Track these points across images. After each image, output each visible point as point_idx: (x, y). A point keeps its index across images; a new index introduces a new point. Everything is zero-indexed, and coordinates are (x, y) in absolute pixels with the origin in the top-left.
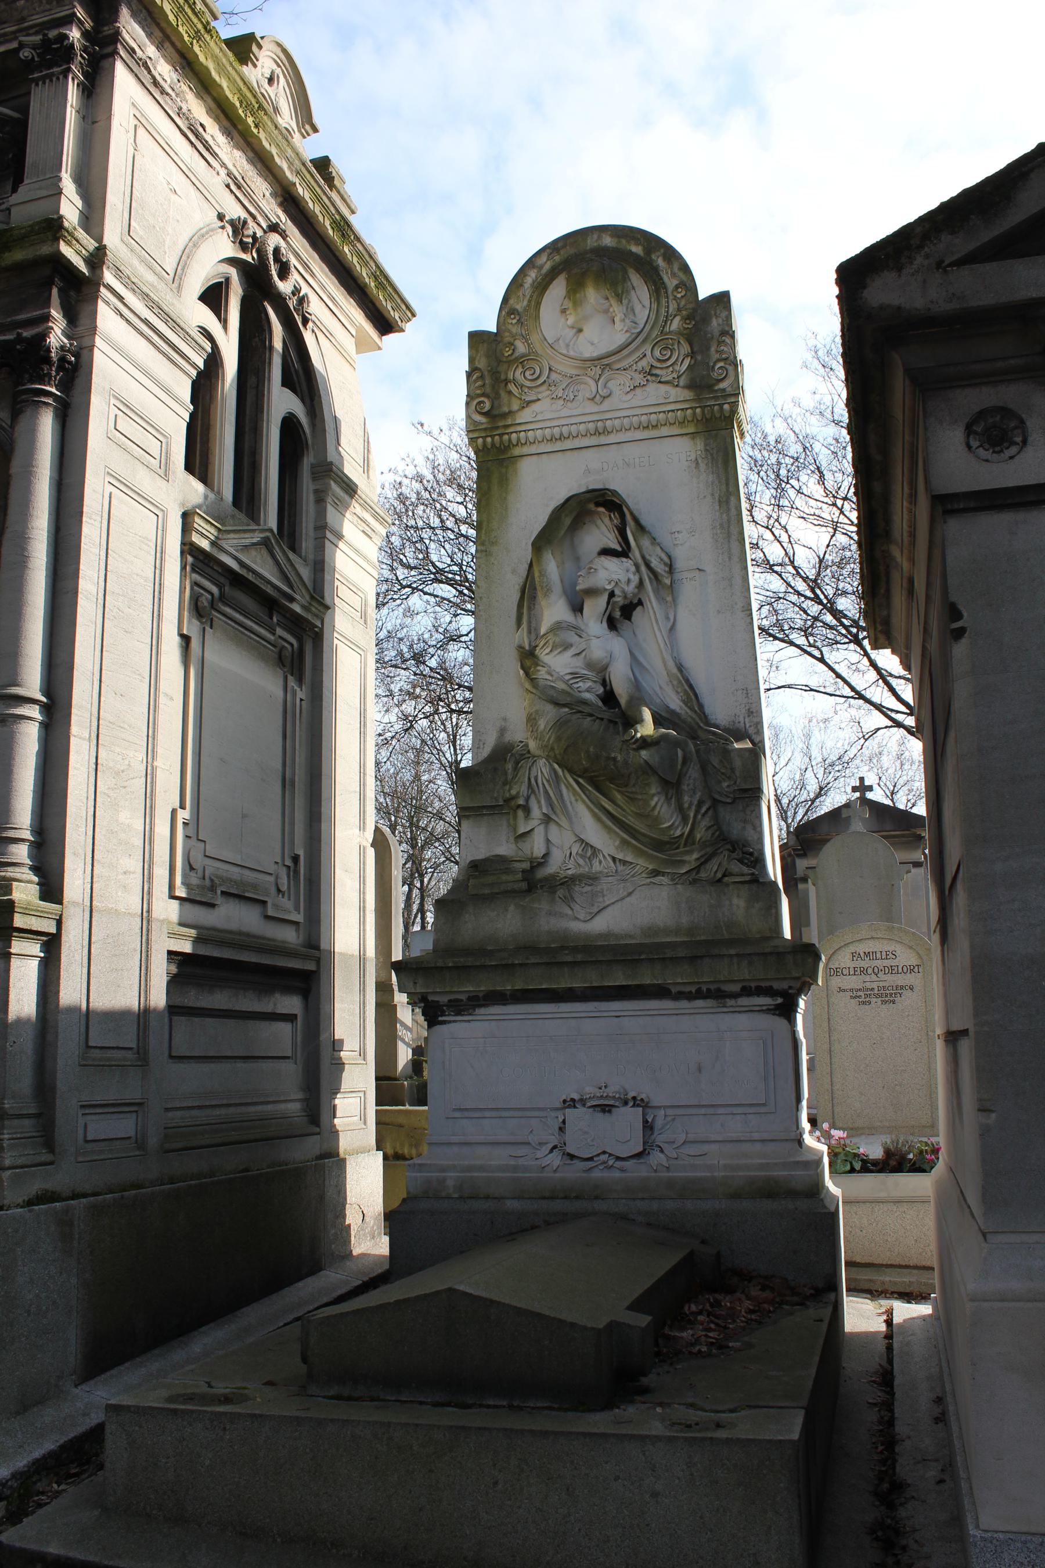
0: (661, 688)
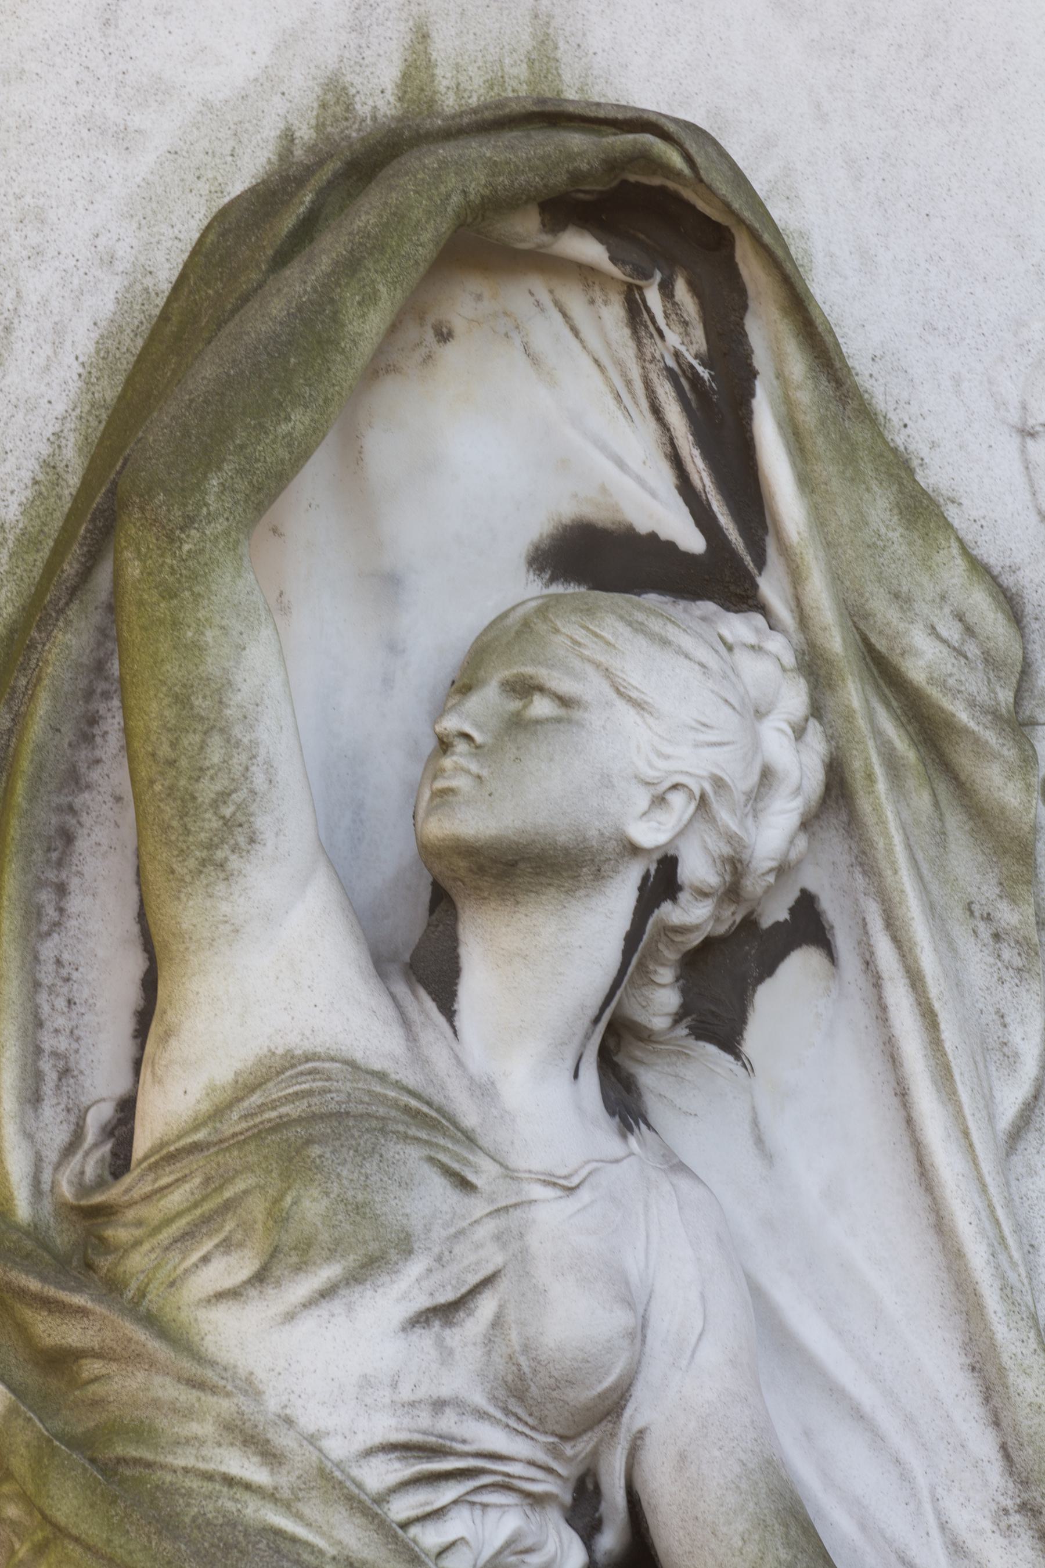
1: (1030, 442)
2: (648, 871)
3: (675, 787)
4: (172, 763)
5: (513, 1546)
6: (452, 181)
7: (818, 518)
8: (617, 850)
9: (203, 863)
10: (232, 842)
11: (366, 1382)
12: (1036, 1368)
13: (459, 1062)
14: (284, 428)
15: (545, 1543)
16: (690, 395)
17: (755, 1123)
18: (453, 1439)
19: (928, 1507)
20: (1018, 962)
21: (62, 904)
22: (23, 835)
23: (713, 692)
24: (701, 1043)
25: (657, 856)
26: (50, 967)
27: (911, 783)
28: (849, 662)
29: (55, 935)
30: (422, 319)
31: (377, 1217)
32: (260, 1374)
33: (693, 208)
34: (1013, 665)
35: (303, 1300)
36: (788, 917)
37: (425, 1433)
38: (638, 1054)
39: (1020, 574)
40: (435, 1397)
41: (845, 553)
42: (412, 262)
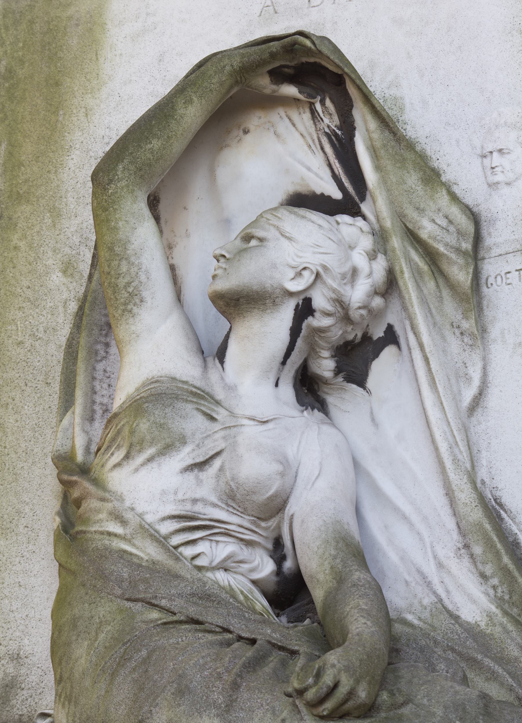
0: (440, 565)
1: (484, 159)
2: (298, 303)
3: (305, 268)
4: (109, 273)
5: (232, 559)
6: (226, 61)
7: (384, 180)
8: (281, 293)
9: (124, 311)
10: (134, 302)
11: (164, 492)
12: (466, 489)
13: (222, 378)
14: (149, 146)
15: (254, 561)
16: (336, 142)
17: (372, 413)
18: (200, 514)
19: (429, 550)
20: (470, 342)
21: (107, 350)
22: (87, 323)
23: (323, 234)
24: (350, 384)
25: (302, 297)
26: (101, 373)
27: (427, 278)
28: (394, 231)
29: (104, 362)
30: (239, 127)
31: (169, 429)
32: (125, 493)
33: (327, 69)
34: (470, 234)
35: (141, 463)
36: (383, 335)
37: (187, 511)
38: (325, 390)
39: (480, 207)
40: (193, 498)
41: (394, 193)
42: (208, 90)
